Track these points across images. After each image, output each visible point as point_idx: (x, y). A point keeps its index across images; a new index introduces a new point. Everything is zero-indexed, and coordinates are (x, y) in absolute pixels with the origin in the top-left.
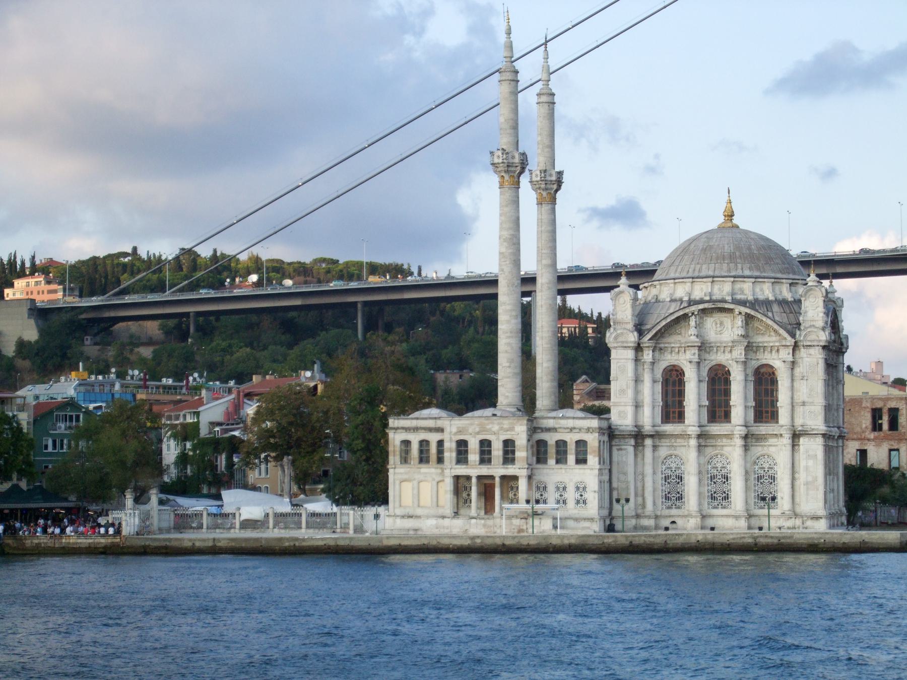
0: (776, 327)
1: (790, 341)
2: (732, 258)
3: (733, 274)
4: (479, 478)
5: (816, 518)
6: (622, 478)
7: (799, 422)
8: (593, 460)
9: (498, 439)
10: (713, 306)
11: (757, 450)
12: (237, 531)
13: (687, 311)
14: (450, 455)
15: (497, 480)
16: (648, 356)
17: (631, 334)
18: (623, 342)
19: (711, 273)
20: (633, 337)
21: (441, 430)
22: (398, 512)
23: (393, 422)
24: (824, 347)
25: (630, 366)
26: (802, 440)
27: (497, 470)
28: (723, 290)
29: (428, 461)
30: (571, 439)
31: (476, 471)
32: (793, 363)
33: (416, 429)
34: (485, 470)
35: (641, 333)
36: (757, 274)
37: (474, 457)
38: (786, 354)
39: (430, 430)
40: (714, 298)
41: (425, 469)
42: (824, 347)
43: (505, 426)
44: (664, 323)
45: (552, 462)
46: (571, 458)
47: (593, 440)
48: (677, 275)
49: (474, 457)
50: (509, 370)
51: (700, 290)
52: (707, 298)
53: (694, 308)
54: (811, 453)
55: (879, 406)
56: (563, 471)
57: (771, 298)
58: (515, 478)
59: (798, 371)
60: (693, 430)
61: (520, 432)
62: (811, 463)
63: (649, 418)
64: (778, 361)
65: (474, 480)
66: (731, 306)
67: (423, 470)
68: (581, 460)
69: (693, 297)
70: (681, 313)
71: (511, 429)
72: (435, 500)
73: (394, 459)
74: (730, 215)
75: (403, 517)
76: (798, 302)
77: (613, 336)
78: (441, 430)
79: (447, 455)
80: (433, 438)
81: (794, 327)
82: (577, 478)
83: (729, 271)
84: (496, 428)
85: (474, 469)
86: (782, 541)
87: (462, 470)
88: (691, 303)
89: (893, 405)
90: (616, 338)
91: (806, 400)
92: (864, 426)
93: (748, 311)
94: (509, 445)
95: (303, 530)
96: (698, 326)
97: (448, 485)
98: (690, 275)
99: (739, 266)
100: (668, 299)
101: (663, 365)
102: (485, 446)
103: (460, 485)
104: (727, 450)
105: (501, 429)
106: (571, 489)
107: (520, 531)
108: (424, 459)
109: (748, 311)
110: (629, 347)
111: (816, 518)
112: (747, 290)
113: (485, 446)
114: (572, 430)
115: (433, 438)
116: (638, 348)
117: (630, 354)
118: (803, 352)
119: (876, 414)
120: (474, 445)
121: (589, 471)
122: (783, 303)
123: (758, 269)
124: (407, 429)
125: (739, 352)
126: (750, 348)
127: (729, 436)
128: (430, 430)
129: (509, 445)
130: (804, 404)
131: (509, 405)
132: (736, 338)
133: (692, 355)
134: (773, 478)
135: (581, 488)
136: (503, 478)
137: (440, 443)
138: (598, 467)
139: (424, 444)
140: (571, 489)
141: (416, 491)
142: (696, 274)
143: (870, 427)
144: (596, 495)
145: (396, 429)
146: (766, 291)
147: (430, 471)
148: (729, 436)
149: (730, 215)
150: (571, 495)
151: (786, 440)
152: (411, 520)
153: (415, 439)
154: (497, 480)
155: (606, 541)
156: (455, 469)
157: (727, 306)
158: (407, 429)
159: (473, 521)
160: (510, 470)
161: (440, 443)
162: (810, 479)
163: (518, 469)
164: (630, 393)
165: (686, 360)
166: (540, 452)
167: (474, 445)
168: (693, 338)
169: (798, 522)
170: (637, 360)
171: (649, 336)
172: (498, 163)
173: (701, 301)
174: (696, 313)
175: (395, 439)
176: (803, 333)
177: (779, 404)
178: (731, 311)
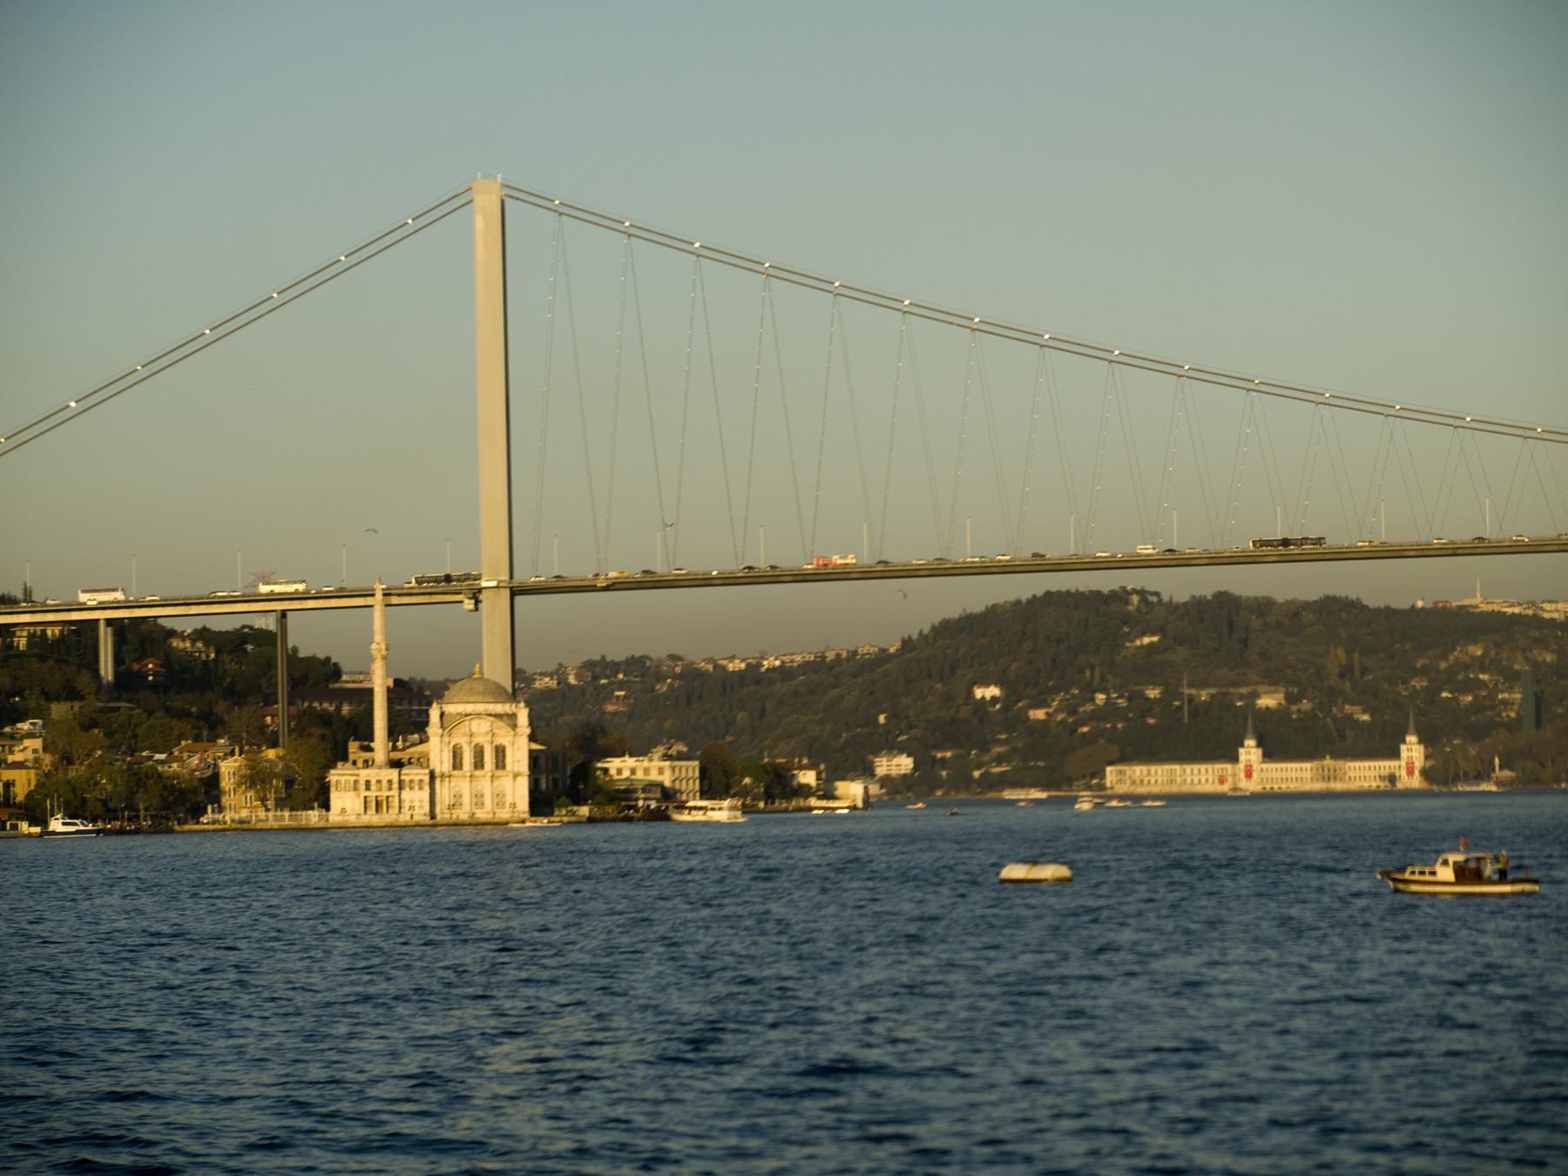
1: (513, 733)
2: (483, 693)
7: (516, 770)
11: (496, 783)
14: (362, 786)
16: (446, 739)
20: (440, 731)
21: (358, 775)
25: (439, 745)
26: (519, 778)
33: (344, 775)
34: (378, 794)
37: (373, 787)
38: (511, 738)
45: (407, 789)
46: (417, 788)
47: (427, 779)
58: (393, 796)
59: (516, 746)
60: (468, 774)
63: (446, 766)
68: (420, 788)
80: (353, 778)
81: (514, 727)
85: (372, 794)
88: (467, 715)
104: (482, 783)
108: (345, 790)
115: (353, 778)
117: (439, 738)
120: (373, 782)
122: (507, 715)
124: (340, 775)
125: (489, 737)
127: (484, 776)
134: (504, 795)
146: (499, 708)
147: (352, 794)
160: (391, 793)
163: (395, 792)
164: (438, 757)
170: (441, 742)
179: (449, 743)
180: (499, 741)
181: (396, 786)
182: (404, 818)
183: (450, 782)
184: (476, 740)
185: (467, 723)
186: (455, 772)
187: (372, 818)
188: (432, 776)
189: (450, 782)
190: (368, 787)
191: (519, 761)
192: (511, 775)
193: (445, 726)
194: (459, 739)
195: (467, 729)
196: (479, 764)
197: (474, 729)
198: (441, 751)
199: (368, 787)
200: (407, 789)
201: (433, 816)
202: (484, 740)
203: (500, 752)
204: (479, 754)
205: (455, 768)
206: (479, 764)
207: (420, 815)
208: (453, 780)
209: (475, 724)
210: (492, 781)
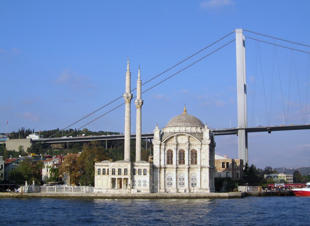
0: (197, 139)
2: (185, 122)
3: (186, 125)
4: (118, 179)
5: (207, 189)
6: (156, 179)
8: (148, 174)
9: (123, 168)
12: (55, 192)
13: (173, 135)
14: (110, 173)
15: (123, 179)
16: (163, 147)
17: (159, 141)
18: (157, 143)
19: (180, 125)
20: (159, 142)
21: (108, 166)
22: (97, 187)
23: (96, 164)
24: (209, 145)
26: (203, 169)
27: (122, 176)
28: (183, 129)
29: (105, 174)
30: (142, 168)
32: (201, 149)
33: (102, 166)
34: (119, 177)
35: (161, 141)
36: (191, 126)
37: (117, 173)
38: (199, 147)
39: (106, 166)
40: (180, 132)
41: (104, 176)
42: (209, 145)
43: (125, 165)
44: (167, 138)
45: (137, 174)
46: (142, 174)
47: (148, 169)
48: (171, 126)
49: (117, 173)
50: (127, 151)
51: (177, 129)
52: (179, 132)
53: (175, 134)
54: (206, 172)
55: (224, 162)
56: (140, 177)
57: (195, 132)
59: (202, 151)
60: (175, 167)
61: (129, 166)
62: (205, 175)
64: (197, 148)
66: (185, 134)
67: (104, 177)
69: (175, 132)
70: (172, 136)
71: (127, 166)
72: (107, 184)
73: (96, 173)
75: (98, 189)
76: (202, 133)
77: (154, 141)
78: (108, 166)
79: (109, 172)
81: (201, 139)
82: (144, 179)
83: (185, 125)
84: (123, 165)
85: (116, 176)
86: (197, 196)
87: (113, 177)
88: (174, 133)
89: (227, 161)
90: (155, 142)
91: (204, 158)
92: (220, 167)
93: (189, 135)
94: (126, 170)
95: (72, 192)
96: (177, 139)
97: (110, 181)
98: (175, 126)
99: (187, 124)
100: (169, 132)
101: (167, 149)
102: (120, 170)
103: (113, 180)
105: (124, 166)
106: (142, 182)
107: (129, 193)
108: (104, 174)
109: (189, 135)
111: (207, 189)
112: (189, 129)
113: (120, 170)
114: (143, 166)
116: (161, 145)
117: (159, 146)
118: (203, 146)
119: (223, 163)
121: (147, 177)
122: (198, 133)
123: (192, 124)
124: (99, 166)
125: (187, 146)
126: (190, 145)
127: (184, 168)
128: (106, 166)
129: (126, 170)
130: (204, 159)
131: (127, 159)
132: (186, 142)
133: (175, 146)
134: (196, 179)
135: (145, 182)
136: (124, 179)
137: (108, 169)
138: (149, 176)
139: (104, 169)
140: (142, 182)
141: (102, 182)
142: (176, 126)
143: (222, 167)
144: (149, 183)
145: (97, 166)
146: (194, 130)
147: (105, 177)
148: (184, 168)
150: (142, 183)
151: (199, 169)
153: (102, 168)
154: (123, 179)
155: (150, 195)
157: (184, 134)
158: (99, 166)
160: (126, 177)
161: (108, 169)
162: (205, 179)
163: (128, 176)
164: (159, 157)
165: (173, 148)
166: (133, 172)
168: (175, 142)
169: (202, 190)
170: (160, 148)
171: (164, 142)
173: (177, 133)
175: (96, 168)
176: (204, 141)
177: (197, 160)
178: (185, 135)
179: (165, 149)
180: (192, 148)
181: (129, 172)
182: (134, 192)
183: (165, 171)
184: (180, 148)
185: (175, 138)
186: (167, 166)
187: (117, 192)
188: (153, 168)
189: (165, 171)
190: (113, 173)
191: (204, 159)
192: (199, 168)
193: (163, 139)
194: (171, 146)
195: (175, 140)
196: (181, 160)
197: (179, 141)
198: (160, 153)
199: (113, 173)
200: (137, 174)
201: (153, 189)
202: (185, 148)
203: (194, 154)
204: (181, 154)
205: (168, 163)
206: (181, 160)
207: (144, 190)
208: (167, 170)
209: (179, 138)
210: (189, 171)
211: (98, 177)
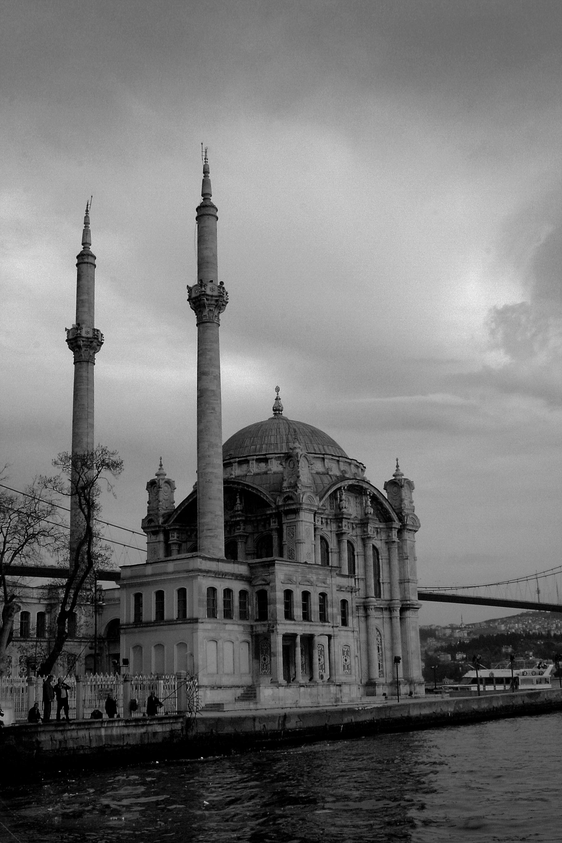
10: (357, 484)
31: (301, 628)
37: (298, 612)
49: (298, 612)
65: (298, 640)
67: (229, 627)
74: (277, 410)
108: (228, 614)
110: (310, 510)
120: (297, 598)
136: (303, 637)
149: (277, 410)
152: (220, 691)
156: (285, 624)
159: (302, 689)
167: (297, 598)
172: (212, 296)
174: (346, 488)
211: (209, 626)
